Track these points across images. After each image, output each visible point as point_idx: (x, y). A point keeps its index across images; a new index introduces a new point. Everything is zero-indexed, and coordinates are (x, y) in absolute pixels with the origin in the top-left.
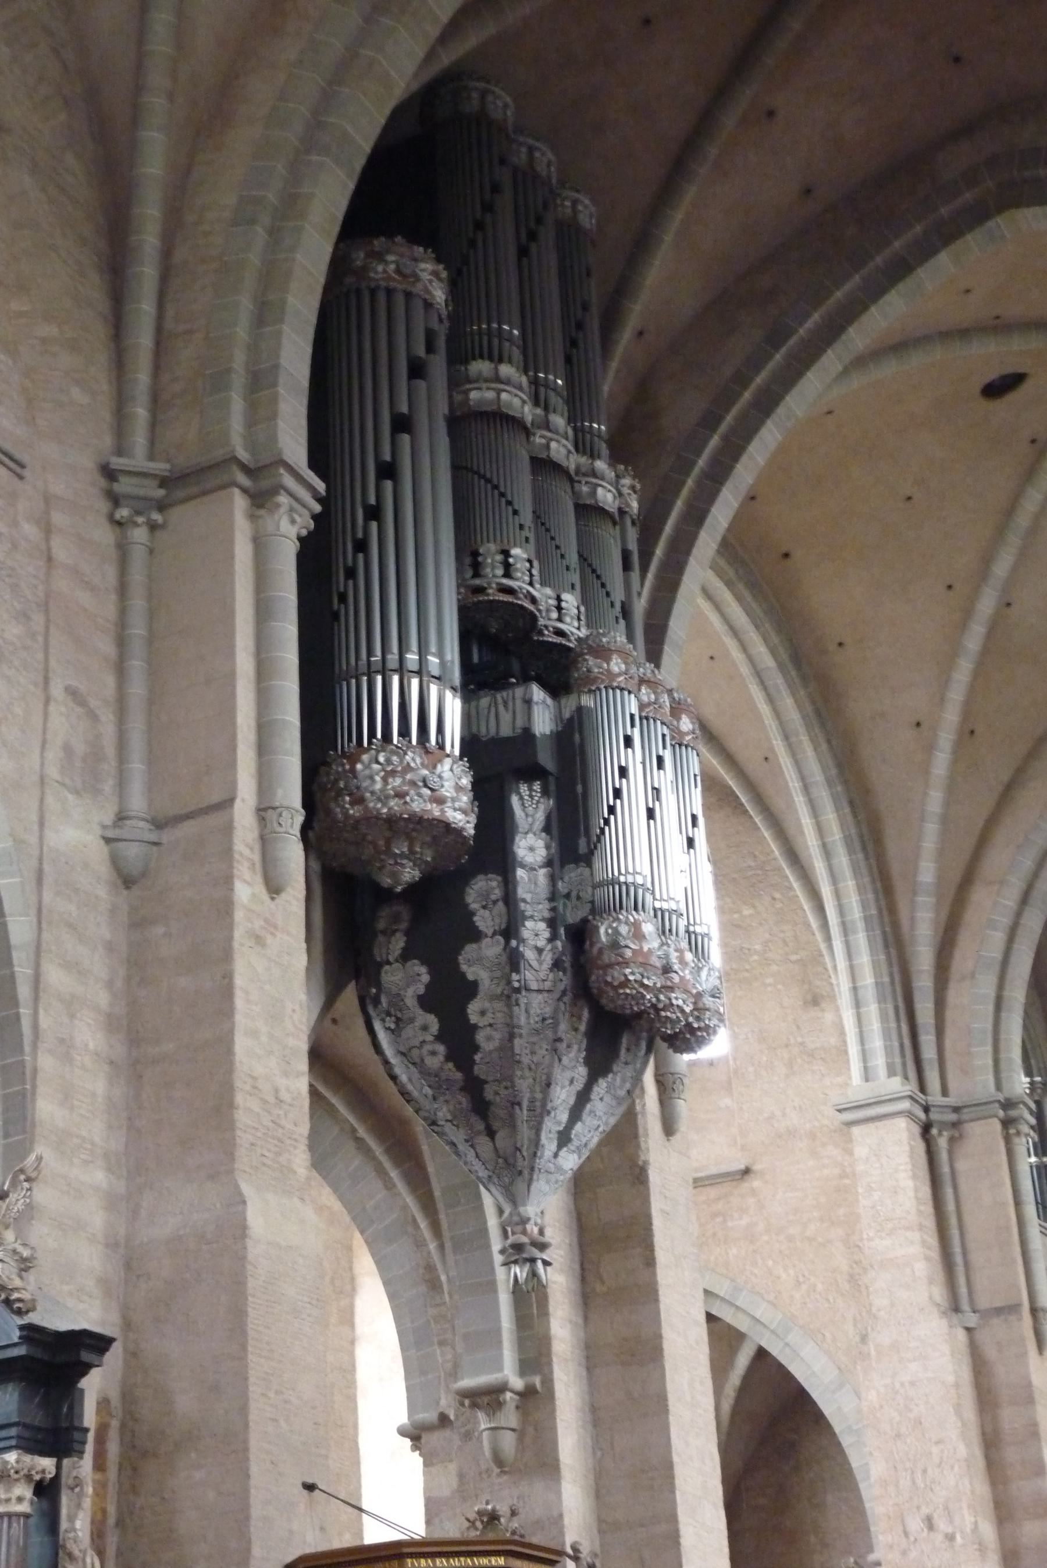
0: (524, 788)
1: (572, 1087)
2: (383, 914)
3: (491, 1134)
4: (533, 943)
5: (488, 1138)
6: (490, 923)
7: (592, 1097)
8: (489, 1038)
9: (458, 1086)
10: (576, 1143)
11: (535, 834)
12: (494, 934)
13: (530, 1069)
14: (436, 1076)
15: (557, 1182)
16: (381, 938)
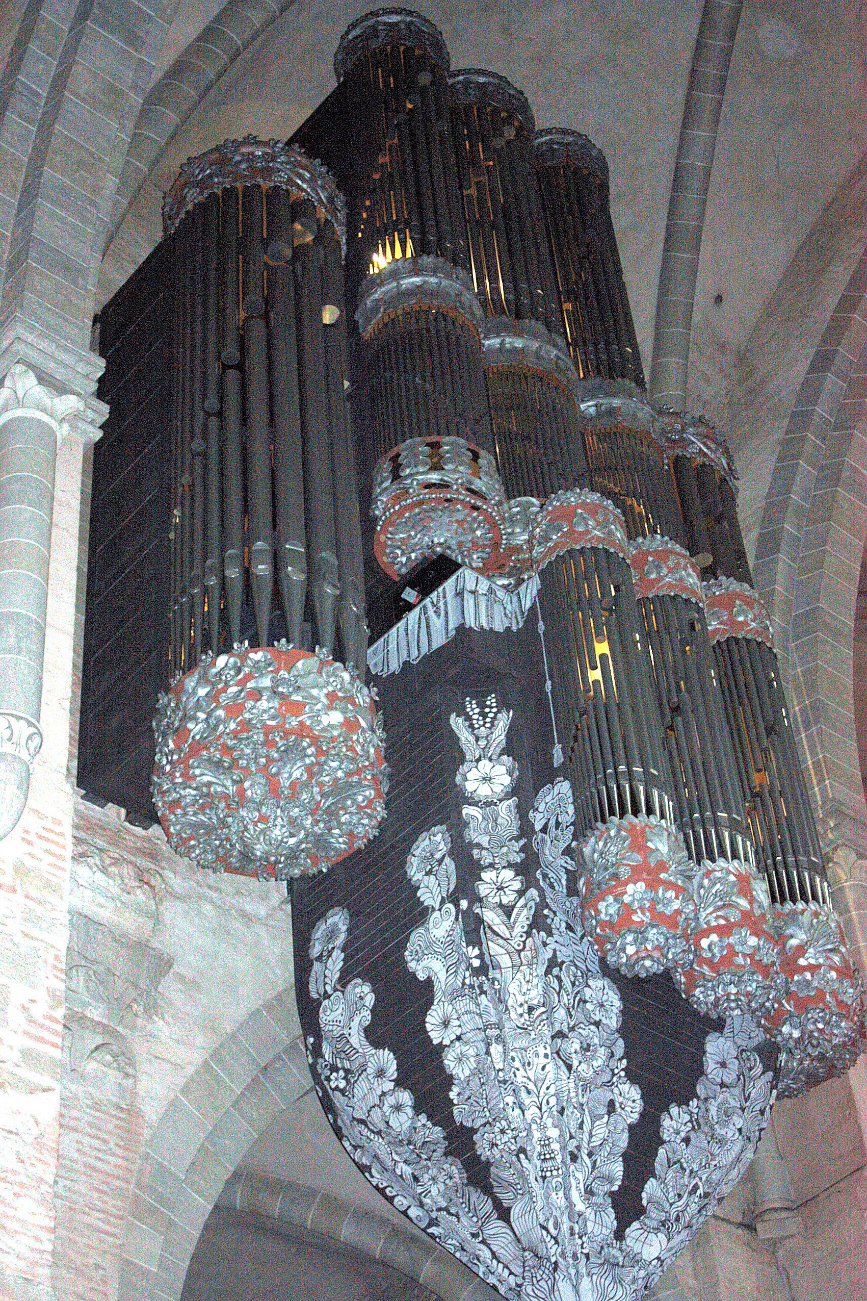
0: (472, 708)
1: (614, 1117)
2: (318, 935)
3: (504, 1214)
4: (497, 899)
5: (501, 1223)
6: (436, 890)
7: (665, 1137)
8: (460, 1059)
9: (440, 1151)
10: (655, 1215)
11: (490, 760)
12: (443, 902)
13: (529, 1092)
14: (409, 1143)
15: (634, 1280)
16: (317, 966)
